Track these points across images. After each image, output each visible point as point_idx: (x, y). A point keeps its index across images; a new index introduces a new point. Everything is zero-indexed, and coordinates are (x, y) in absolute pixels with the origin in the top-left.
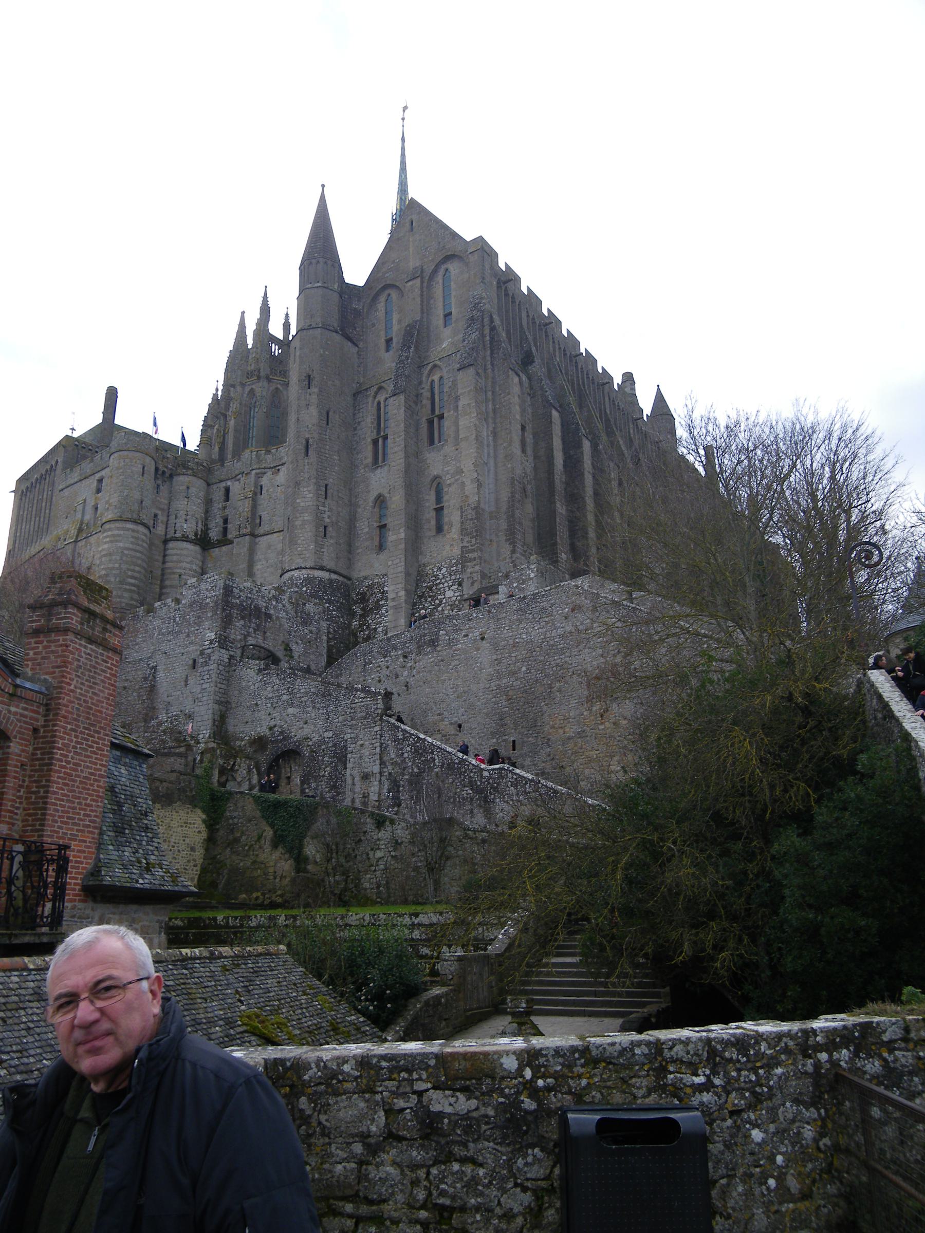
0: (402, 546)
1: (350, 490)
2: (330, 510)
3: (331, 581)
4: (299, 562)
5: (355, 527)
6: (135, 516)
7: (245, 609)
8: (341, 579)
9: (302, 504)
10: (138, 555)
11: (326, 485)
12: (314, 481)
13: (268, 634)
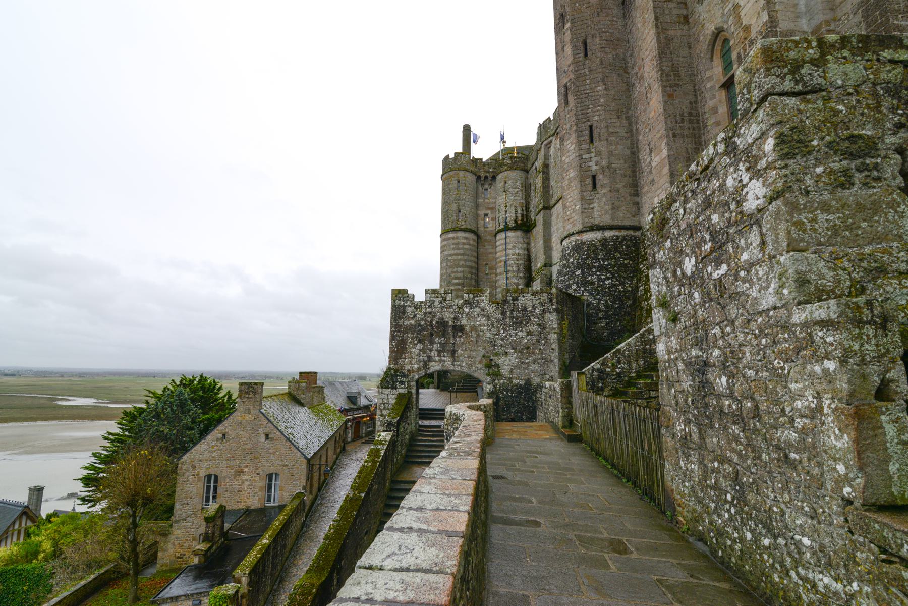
0: (666, 170)
1: (628, 118)
2: (599, 154)
3: (604, 242)
4: (570, 228)
5: (639, 160)
6: (454, 225)
7: (423, 329)
8: (623, 233)
9: (567, 161)
10: (460, 257)
11: (591, 127)
12: (574, 128)
13: (460, 352)
